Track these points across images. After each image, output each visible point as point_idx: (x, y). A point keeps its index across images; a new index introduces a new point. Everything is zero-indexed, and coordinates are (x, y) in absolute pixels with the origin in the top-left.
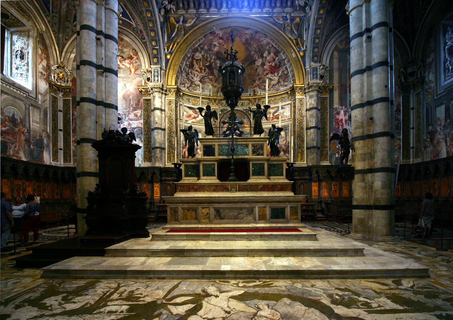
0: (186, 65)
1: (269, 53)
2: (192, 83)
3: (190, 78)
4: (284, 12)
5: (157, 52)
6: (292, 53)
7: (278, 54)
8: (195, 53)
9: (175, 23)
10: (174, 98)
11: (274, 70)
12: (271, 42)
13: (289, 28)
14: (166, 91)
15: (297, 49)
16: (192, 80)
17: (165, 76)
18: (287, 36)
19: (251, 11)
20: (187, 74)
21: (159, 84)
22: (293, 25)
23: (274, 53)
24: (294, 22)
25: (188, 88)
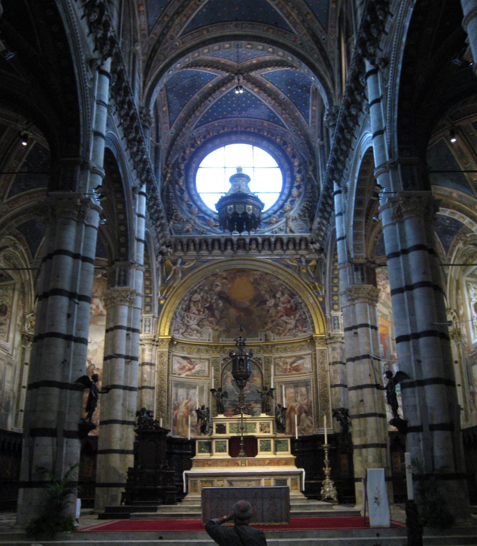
0: (182, 308)
1: (283, 294)
2: (188, 327)
3: (186, 322)
4: (297, 254)
5: (151, 299)
6: (308, 299)
7: (294, 297)
8: (193, 295)
9: (172, 265)
10: (167, 350)
11: (290, 311)
12: (284, 284)
13: (304, 271)
14: (158, 342)
15: (314, 293)
16: (189, 324)
17: (157, 324)
18: (303, 280)
19: (260, 253)
20: (183, 318)
21: (151, 335)
22: (309, 268)
23: (289, 295)
24: (311, 264)
25: (182, 334)
